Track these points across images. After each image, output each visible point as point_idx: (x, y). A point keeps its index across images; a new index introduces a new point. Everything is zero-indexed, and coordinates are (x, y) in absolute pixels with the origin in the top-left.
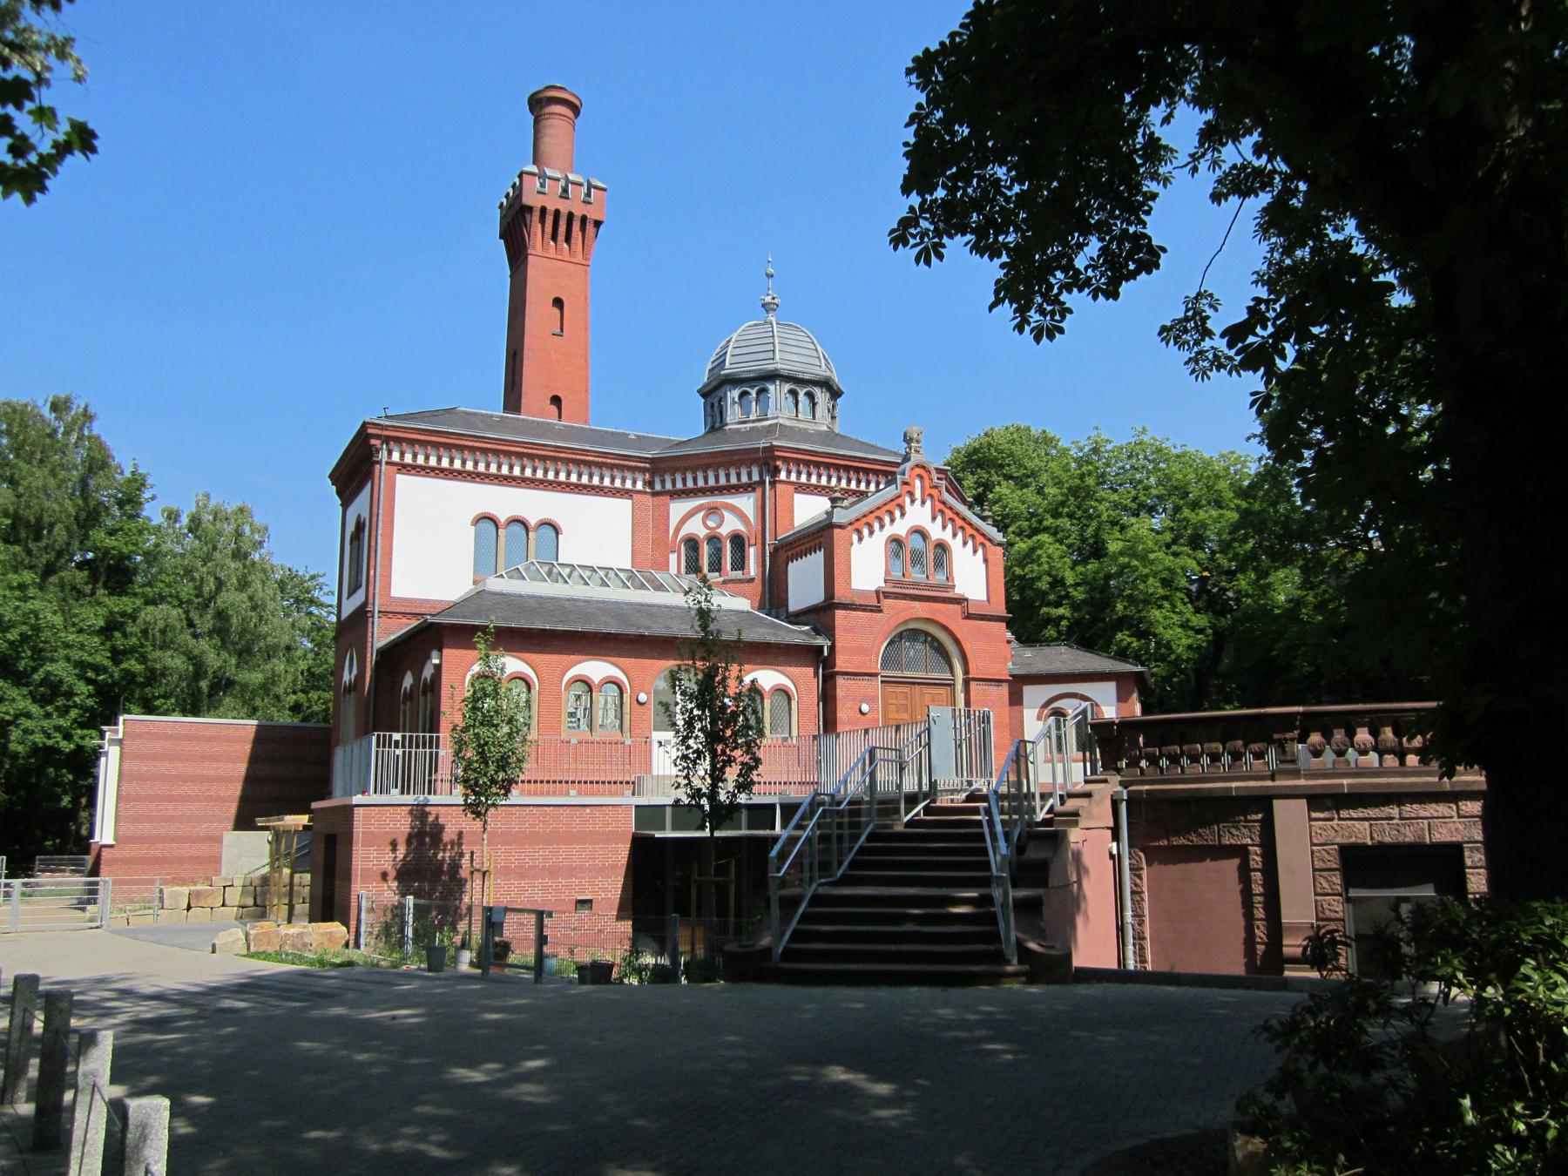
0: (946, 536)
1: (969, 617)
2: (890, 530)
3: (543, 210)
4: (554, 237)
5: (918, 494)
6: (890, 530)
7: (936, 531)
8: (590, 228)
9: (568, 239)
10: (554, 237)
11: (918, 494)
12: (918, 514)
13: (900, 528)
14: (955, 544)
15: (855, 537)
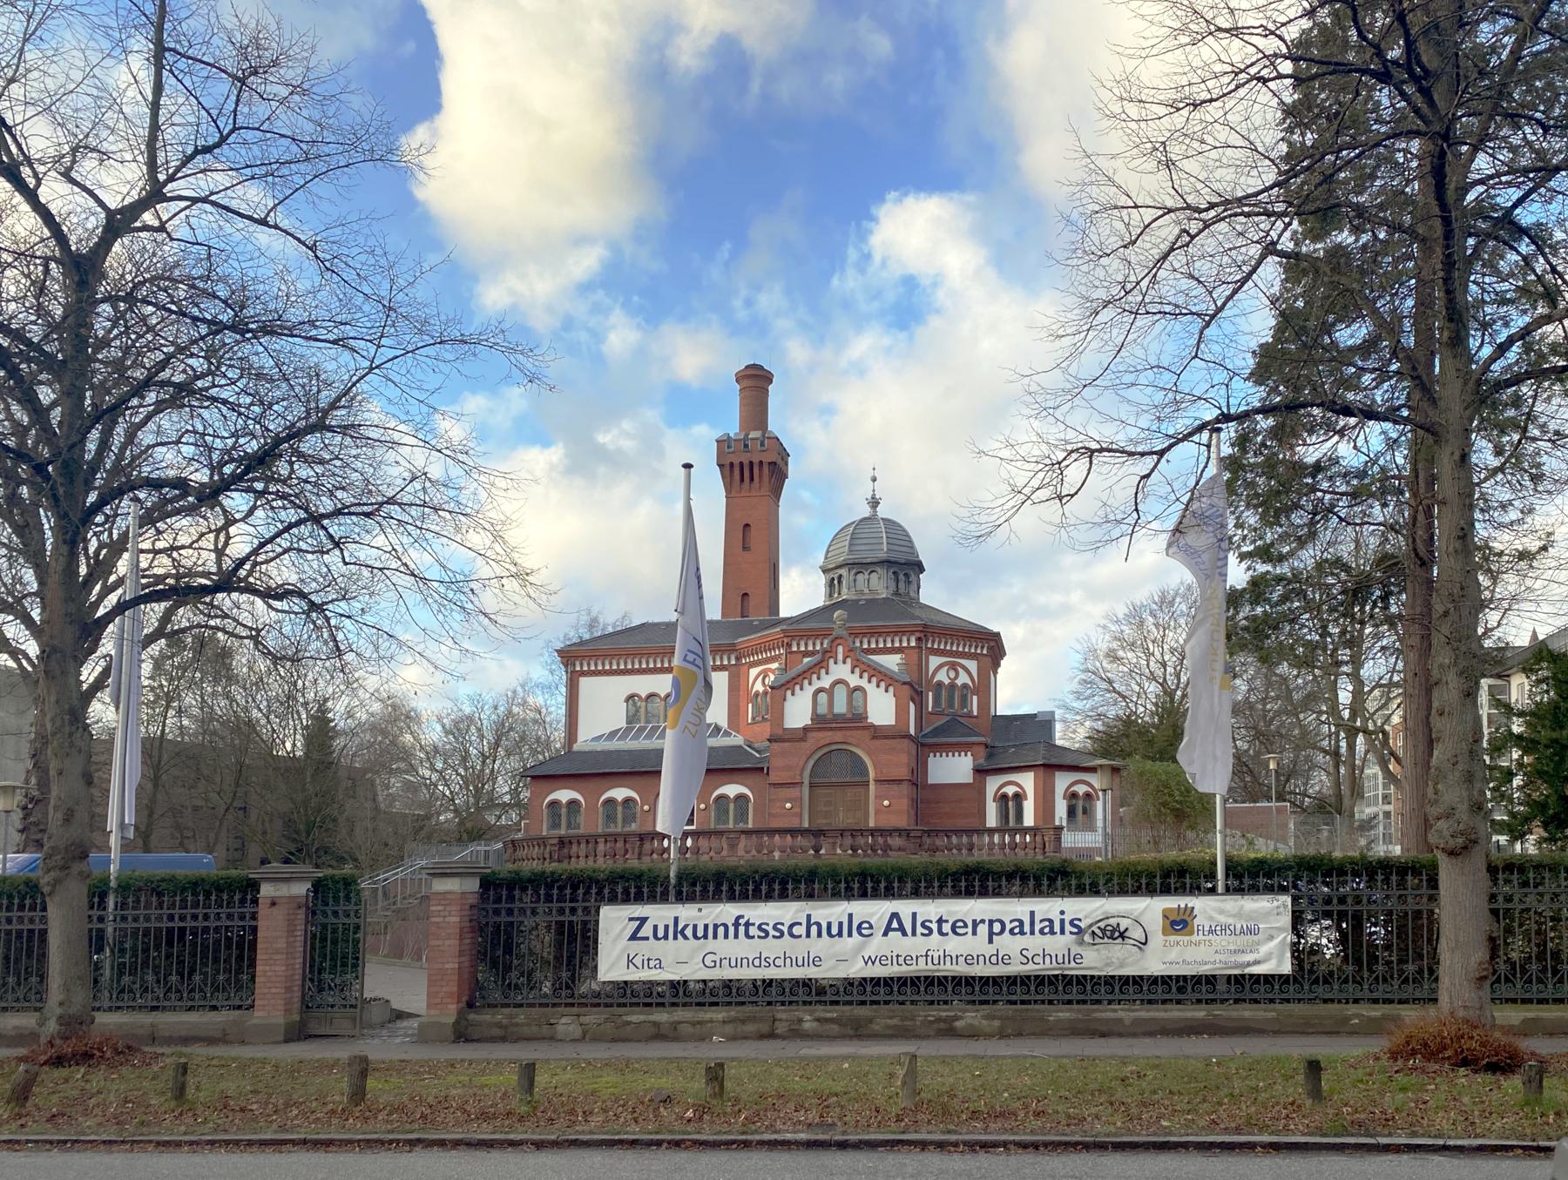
0: (863, 683)
1: (874, 738)
2: (817, 684)
3: (732, 465)
4: (742, 480)
5: (840, 657)
6: (817, 684)
7: (854, 680)
8: (766, 469)
9: (752, 479)
10: (742, 480)
11: (840, 657)
12: (841, 670)
13: (826, 682)
14: (871, 688)
15: (789, 693)
